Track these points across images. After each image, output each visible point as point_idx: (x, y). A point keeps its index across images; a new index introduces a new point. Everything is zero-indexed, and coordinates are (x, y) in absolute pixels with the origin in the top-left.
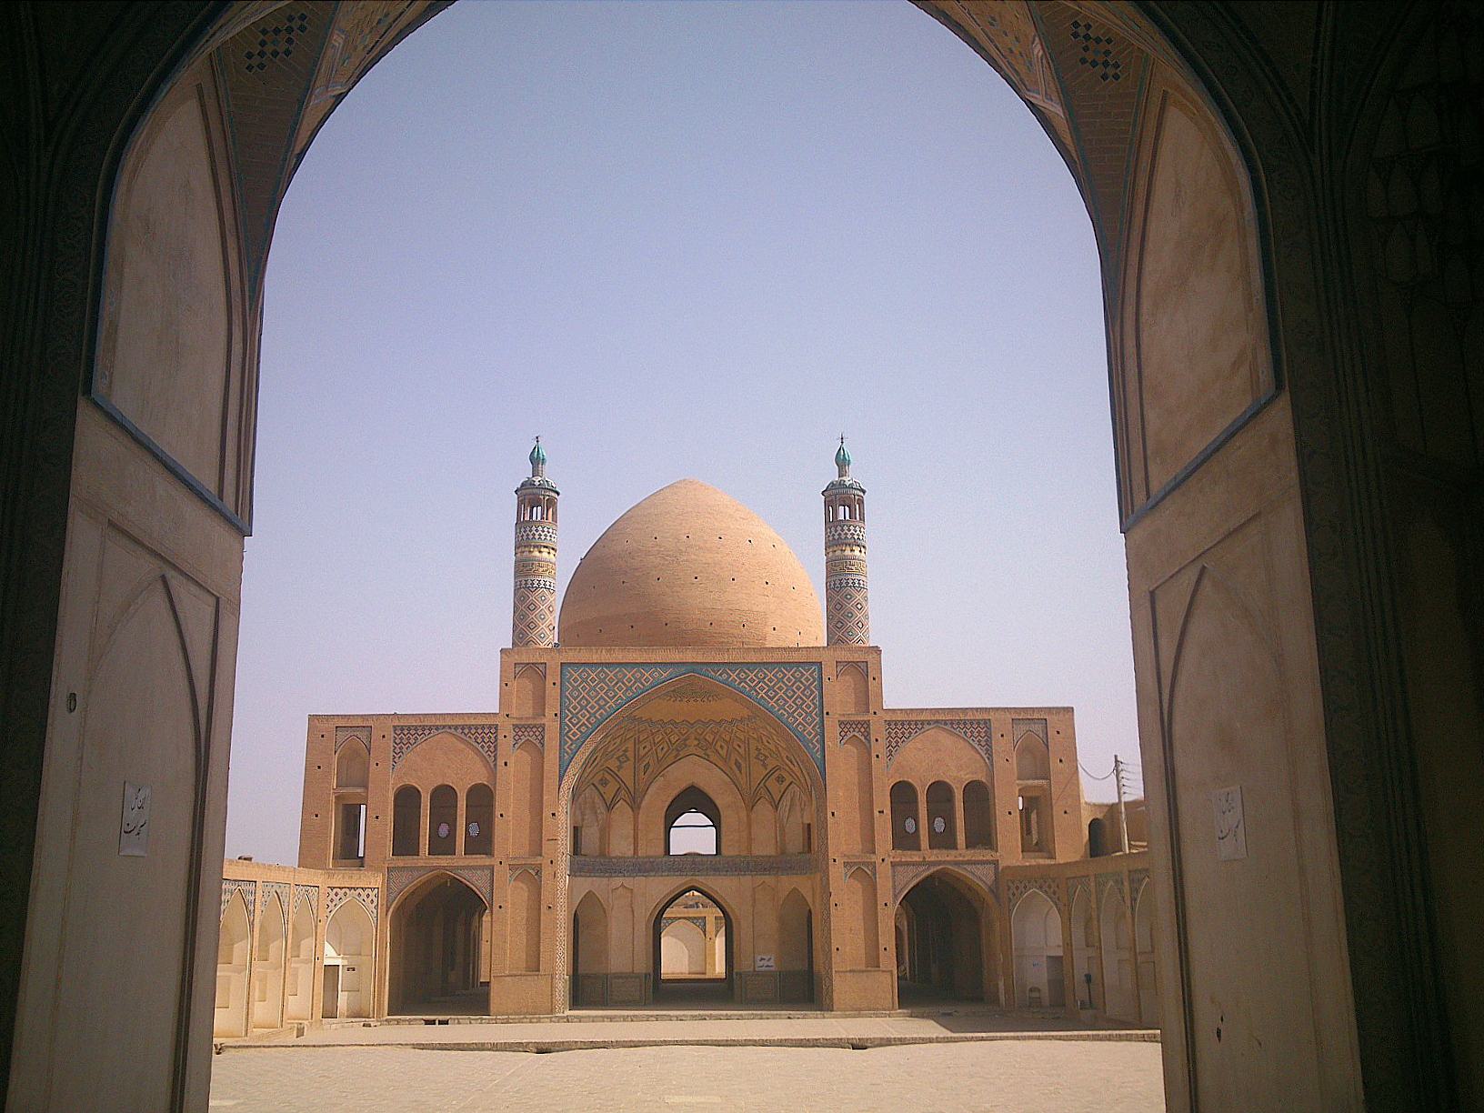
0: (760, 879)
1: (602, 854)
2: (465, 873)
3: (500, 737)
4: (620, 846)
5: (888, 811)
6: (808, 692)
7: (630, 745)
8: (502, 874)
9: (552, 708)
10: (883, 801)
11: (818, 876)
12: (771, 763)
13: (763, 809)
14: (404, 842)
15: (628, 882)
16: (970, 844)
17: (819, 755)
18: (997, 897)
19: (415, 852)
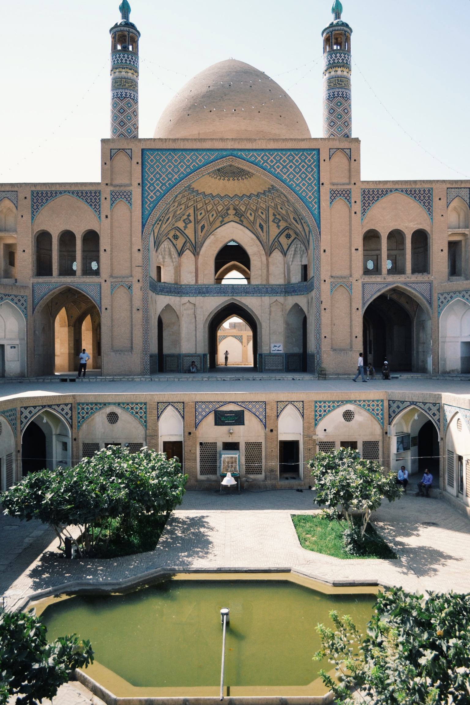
0: (275, 298)
1: (176, 284)
2: (82, 287)
3: (103, 199)
4: (187, 279)
5: (361, 249)
6: (309, 170)
7: (191, 211)
8: (106, 288)
9: (137, 178)
10: (358, 242)
11: (313, 293)
12: (283, 225)
13: (277, 255)
14: (43, 268)
15: (192, 299)
16: (414, 271)
17: (316, 212)
18: (430, 304)
19: (49, 273)
